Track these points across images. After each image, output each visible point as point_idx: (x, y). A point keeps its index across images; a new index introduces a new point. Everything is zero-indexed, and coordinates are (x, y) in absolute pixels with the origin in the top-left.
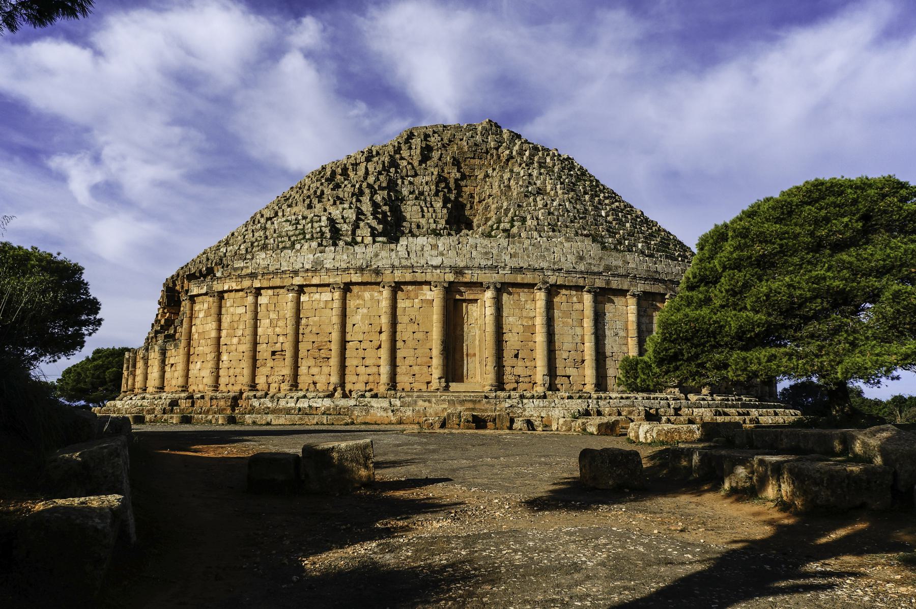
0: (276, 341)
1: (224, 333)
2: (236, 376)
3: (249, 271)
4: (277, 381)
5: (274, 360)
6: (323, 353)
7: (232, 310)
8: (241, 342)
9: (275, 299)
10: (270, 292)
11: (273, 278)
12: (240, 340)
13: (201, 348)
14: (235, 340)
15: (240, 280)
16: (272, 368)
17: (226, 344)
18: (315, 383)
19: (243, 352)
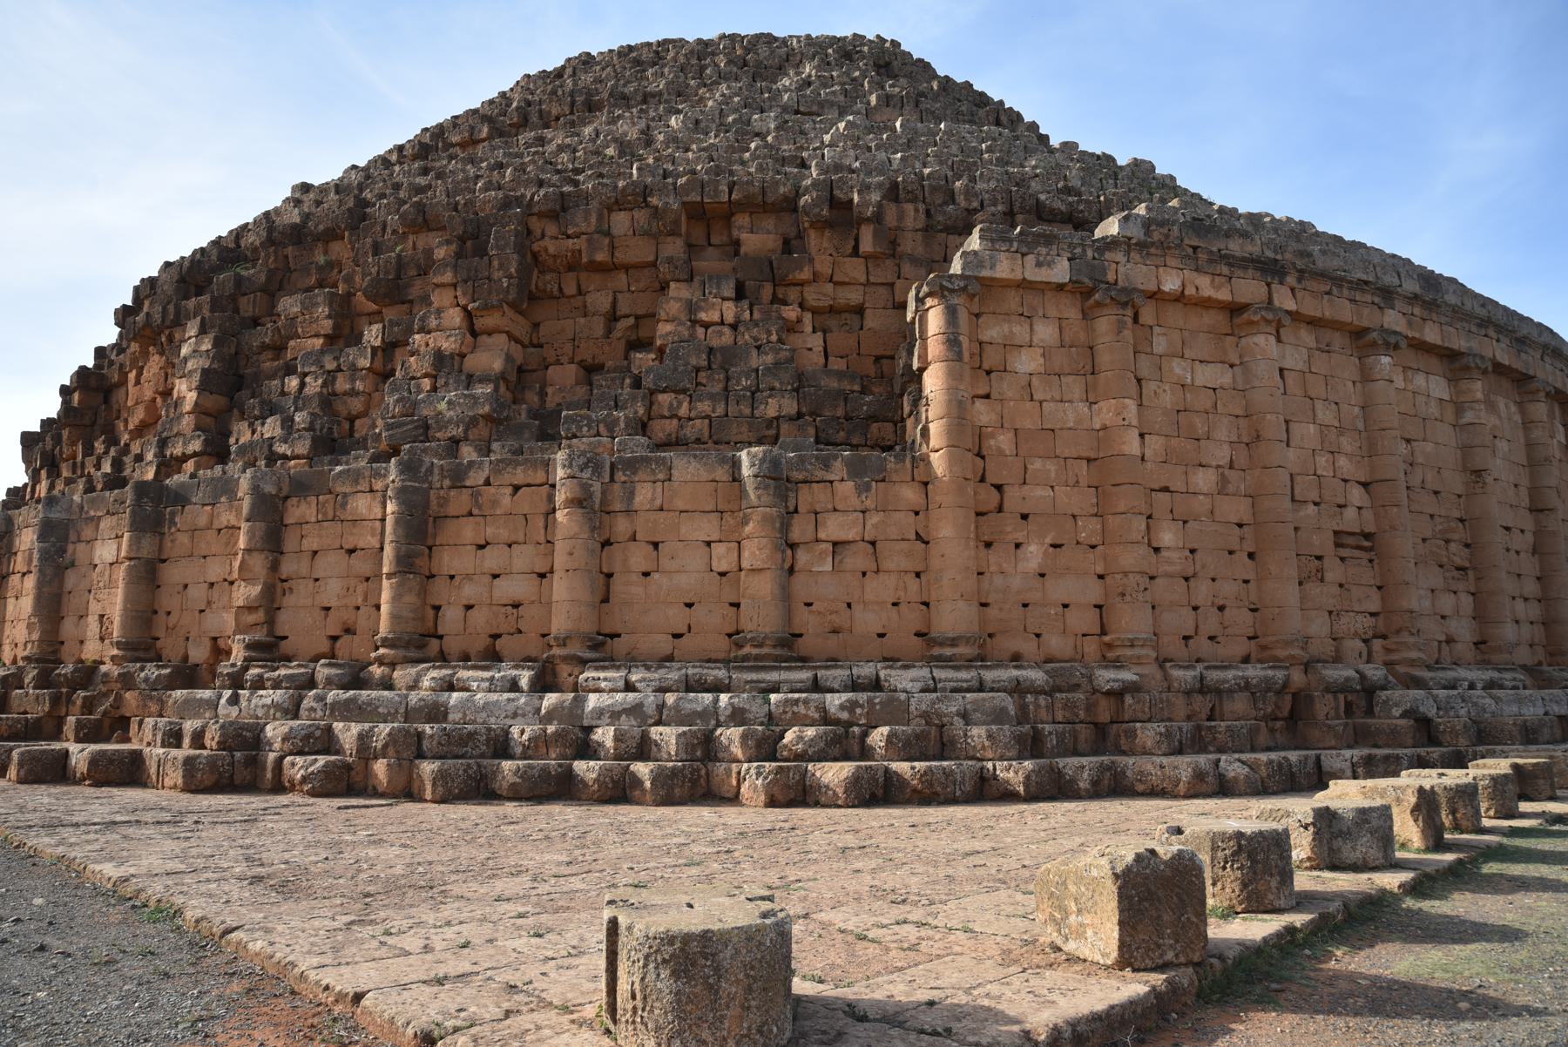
0: (1341, 501)
1: (1155, 444)
2: (1221, 608)
3: (1254, 249)
4: (1361, 631)
5: (1342, 559)
6: (1459, 555)
7: (1178, 368)
8: (1231, 488)
9: (1321, 364)
10: (1307, 337)
11: (1328, 293)
12: (1223, 481)
13: (1041, 492)
14: (1204, 480)
15: (1225, 270)
16: (1341, 586)
17: (1166, 489)
18: (1450, 641)
19: (1240, 526)
